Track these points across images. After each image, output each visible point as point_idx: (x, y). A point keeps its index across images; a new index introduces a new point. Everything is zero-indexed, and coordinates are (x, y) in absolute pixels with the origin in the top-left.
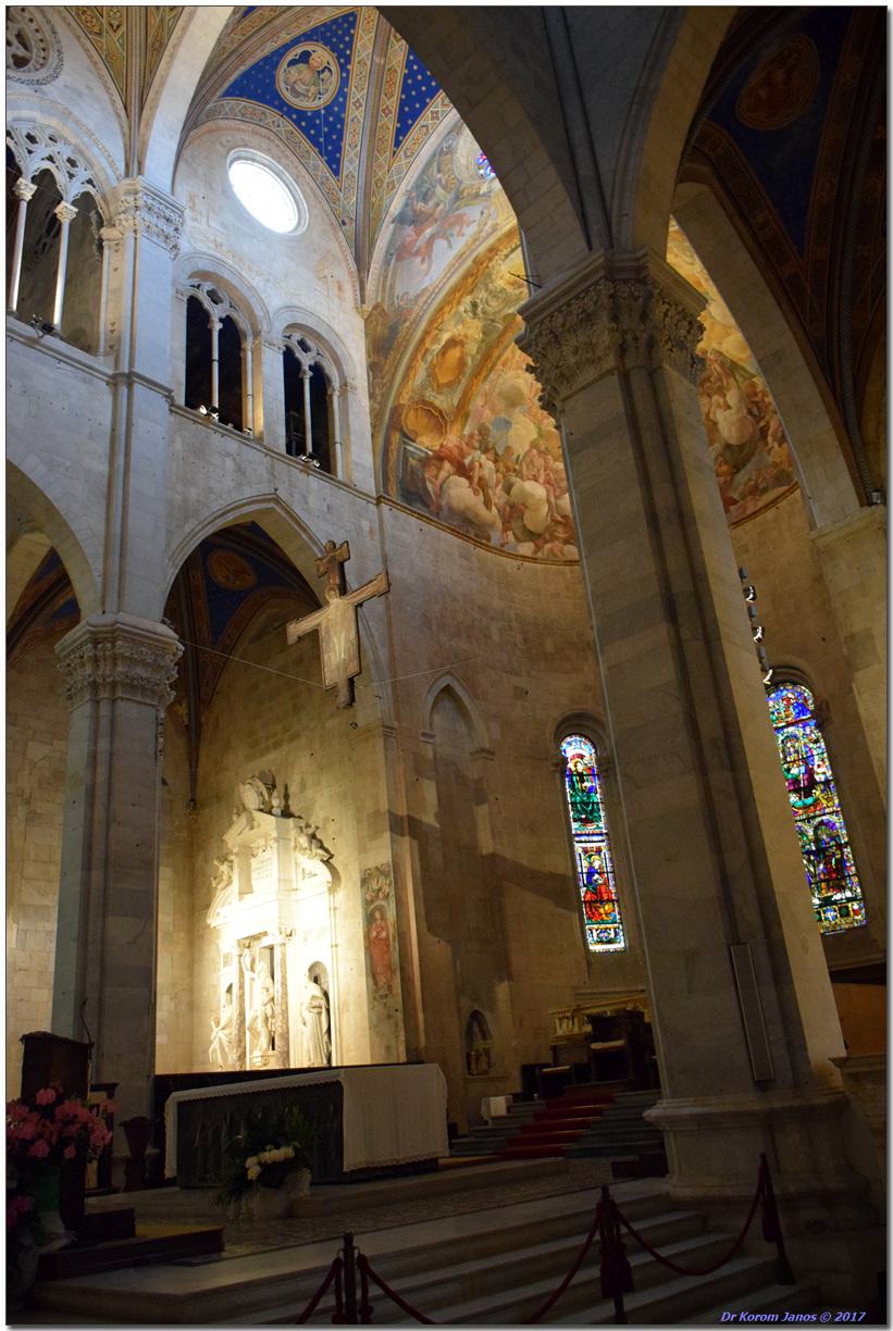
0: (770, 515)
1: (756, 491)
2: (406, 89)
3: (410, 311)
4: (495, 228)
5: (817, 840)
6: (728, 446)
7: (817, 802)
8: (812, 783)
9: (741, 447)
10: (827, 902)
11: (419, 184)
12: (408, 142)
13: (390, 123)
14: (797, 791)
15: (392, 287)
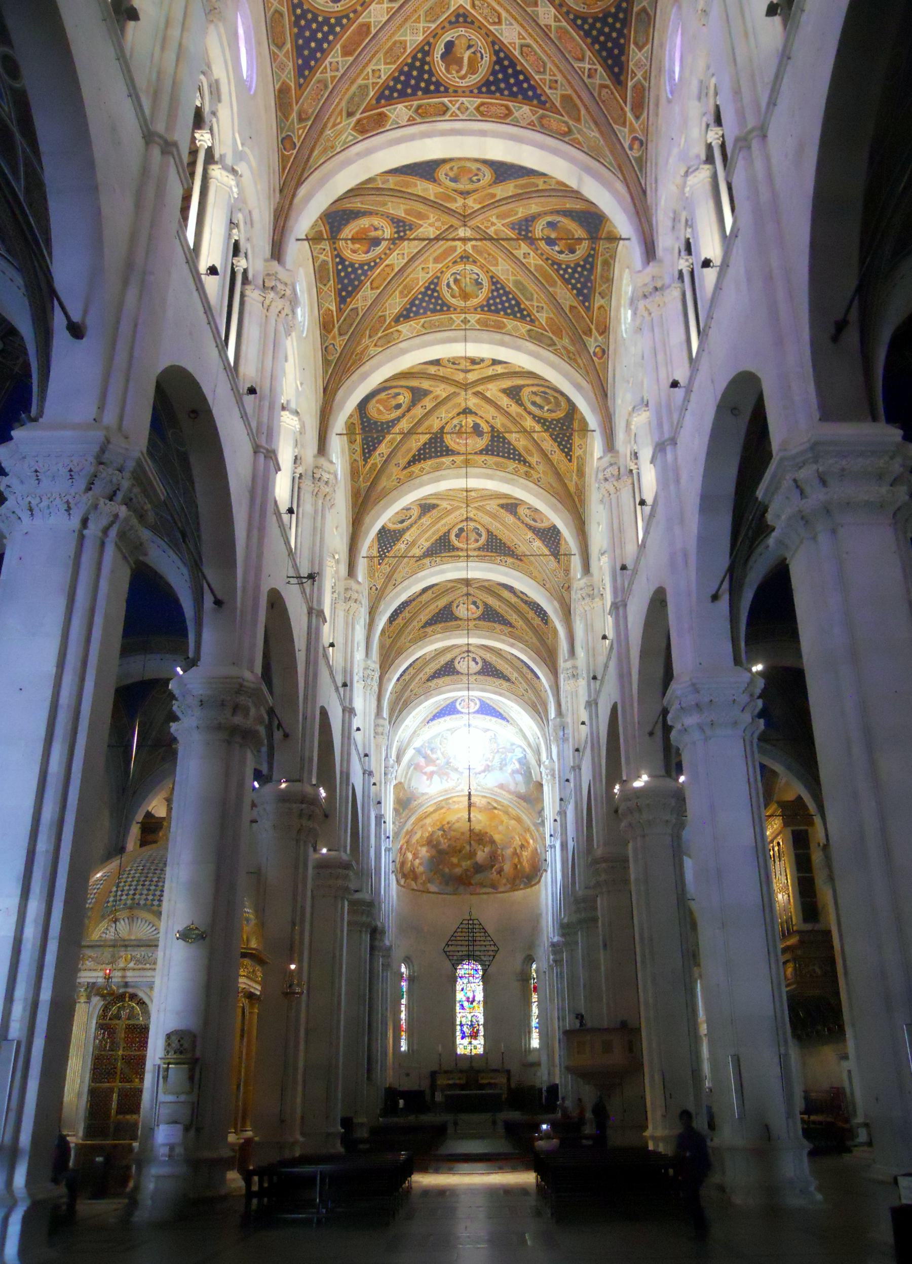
0: (485, 896)
1: (482, 885)
2: (442, 710)
3: (418, 798)
4: (462, 790)
5: (471, 1021)
6: (476, 863)
7: (474, 1008)
8: (473, 1001)
9: (481, 866)
10: (470, 1043)
11: (430, 742)
12: (431, 724)
13: (430, 717)
14: (468, 1001)
15: (410, 780)
